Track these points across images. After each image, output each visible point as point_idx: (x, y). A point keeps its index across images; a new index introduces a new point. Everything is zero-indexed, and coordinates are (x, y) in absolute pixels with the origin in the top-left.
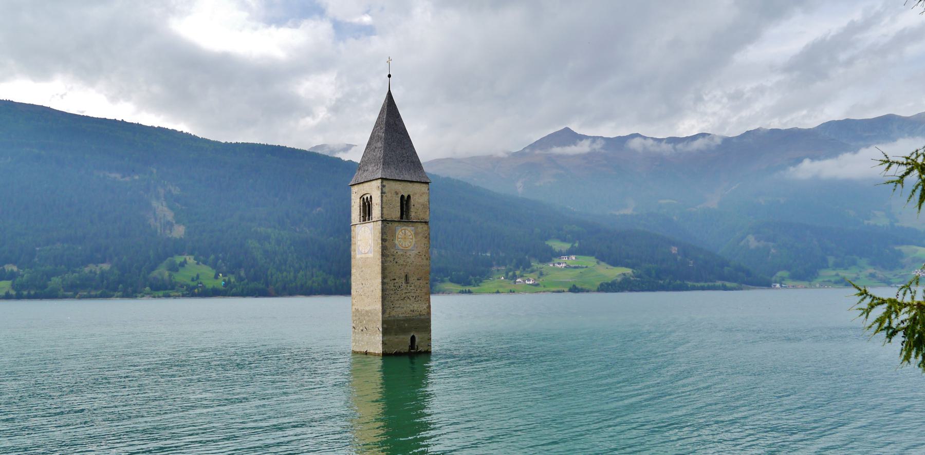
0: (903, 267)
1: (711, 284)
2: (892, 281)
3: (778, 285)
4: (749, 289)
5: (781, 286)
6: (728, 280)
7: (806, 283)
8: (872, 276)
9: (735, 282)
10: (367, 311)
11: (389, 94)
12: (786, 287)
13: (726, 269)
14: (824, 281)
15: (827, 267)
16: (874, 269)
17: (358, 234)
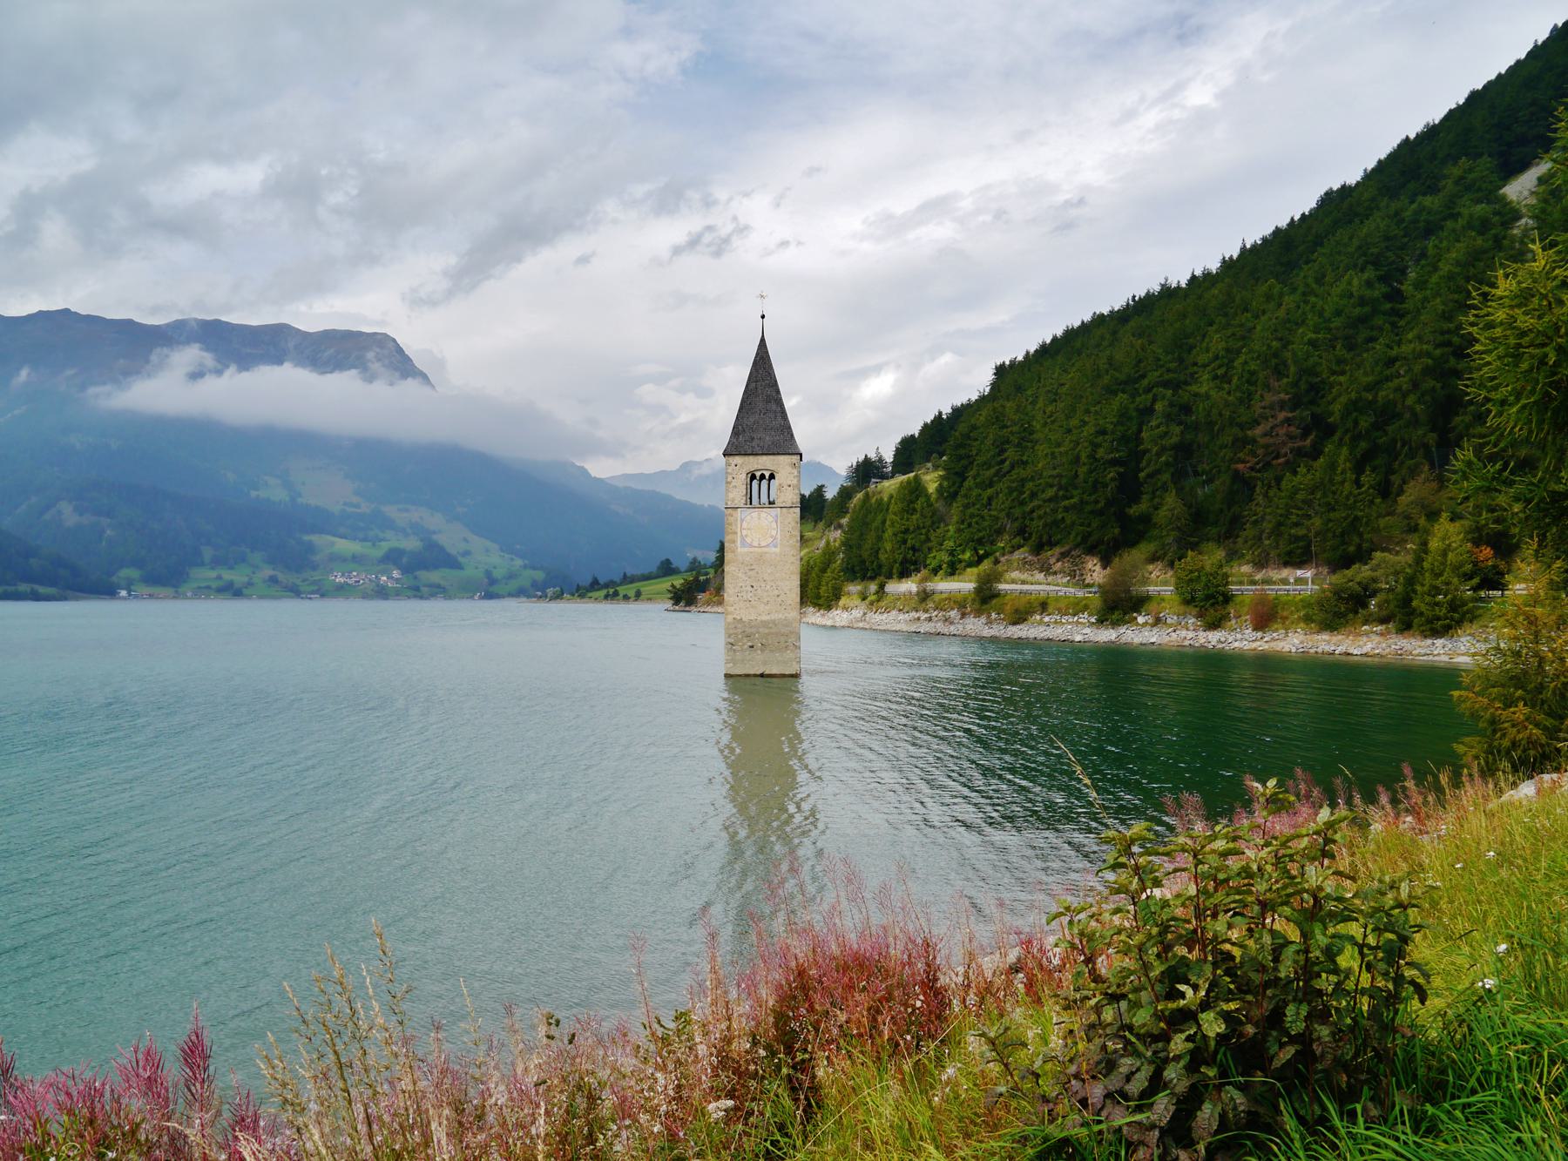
0: (314, 568)
1: (11, 589)
2: (302, 589)
3: (124, 593)
4: (77, 599)
5: (130, 595)
6: (42, 583)
7: (169, 591)
8: (273, 580)
9: (53, 584)
10: (762, 621)
11: (763, 340)
12: (136, 597)
13: (33, 561)
14: (199, 588)
15: (202, 564)
16: (274, 569)
17: (742, 520)
